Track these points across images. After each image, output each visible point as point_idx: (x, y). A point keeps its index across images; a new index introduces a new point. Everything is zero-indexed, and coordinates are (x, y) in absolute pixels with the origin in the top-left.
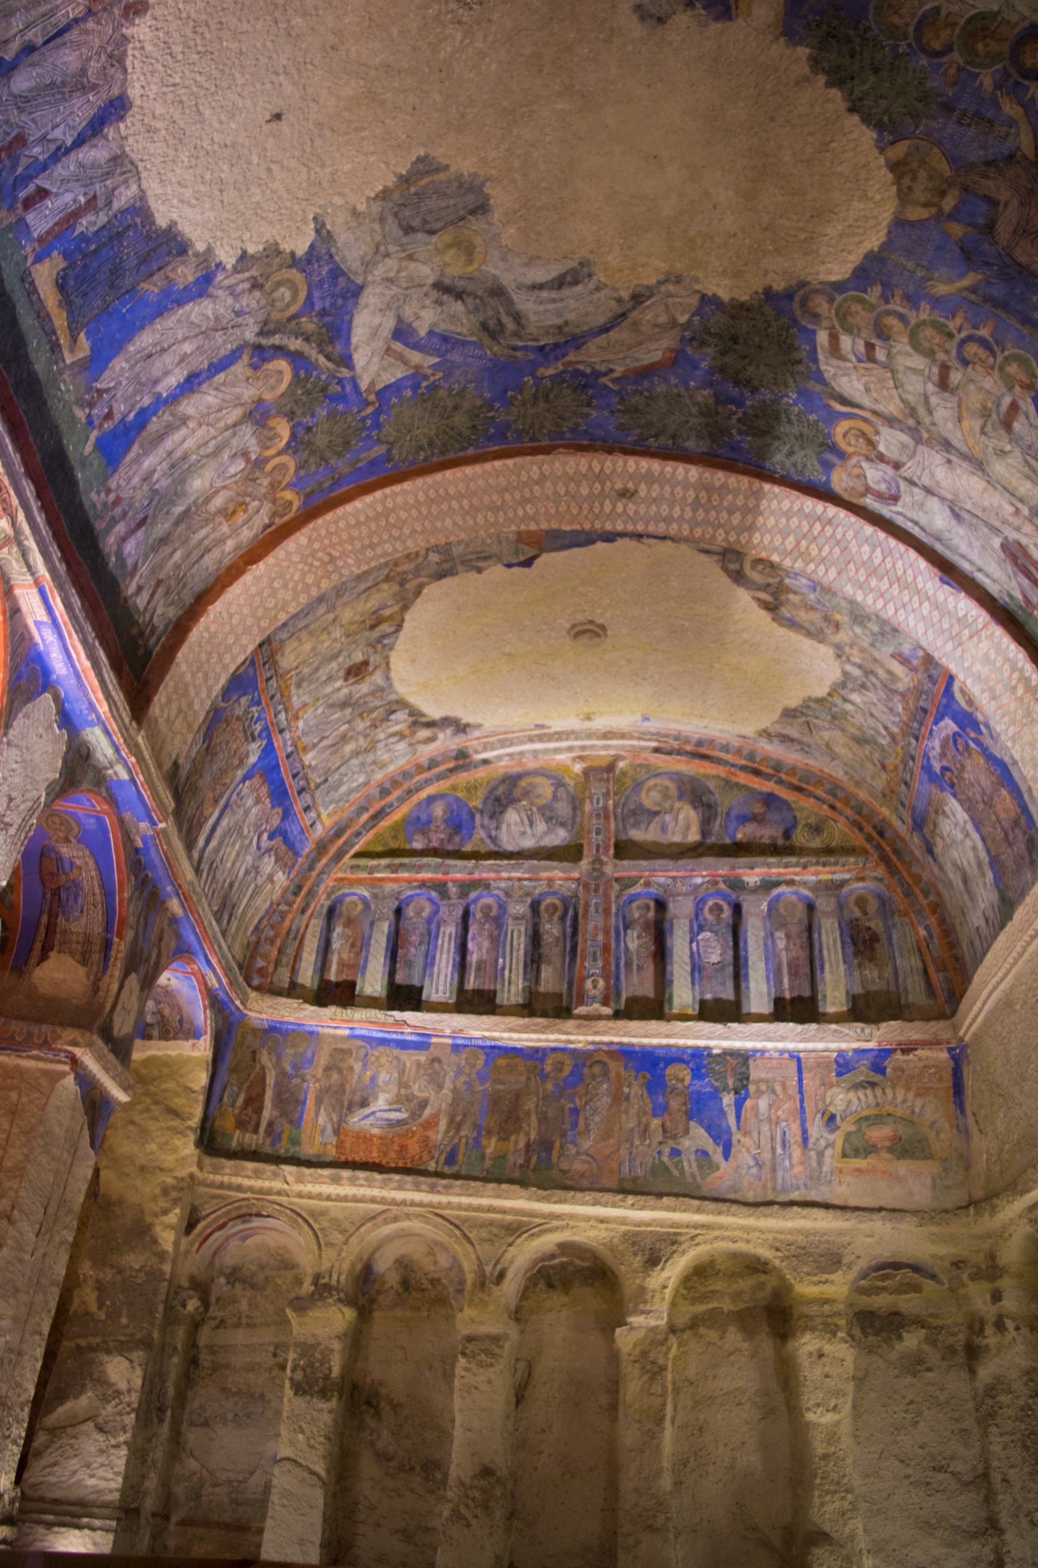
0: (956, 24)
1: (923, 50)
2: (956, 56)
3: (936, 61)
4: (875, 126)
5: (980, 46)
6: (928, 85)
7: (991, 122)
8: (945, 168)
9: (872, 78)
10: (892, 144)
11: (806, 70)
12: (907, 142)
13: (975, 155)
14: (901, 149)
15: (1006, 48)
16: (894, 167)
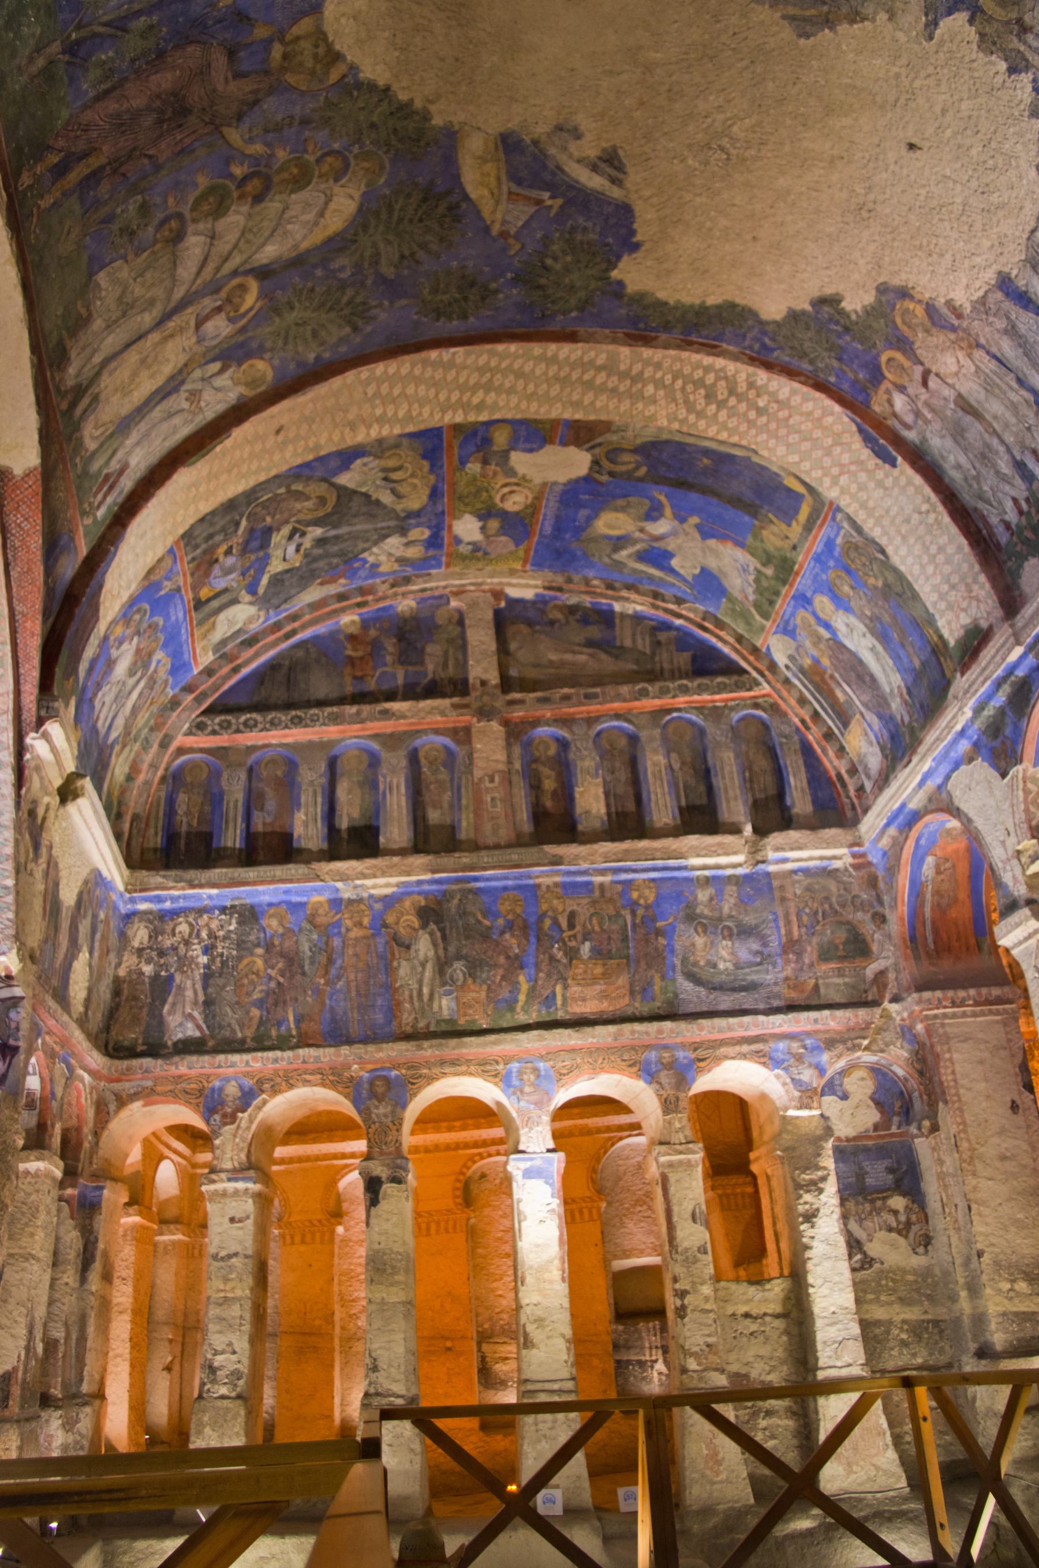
0: (320, 177)
1: (339, 152)
2: (311, 158)
3: (326, 150)
4: (363, 84)
5: (295, 171)
6: (327, 131)
7: (266, 131)
8: (290, 78)
9: (375, 118)
10: (344, 76)
11: (433, 108)
12: (331, 82)
13: (270, 104)
14: (334, 76)
15: (276, 179)
16: (337, 57)
